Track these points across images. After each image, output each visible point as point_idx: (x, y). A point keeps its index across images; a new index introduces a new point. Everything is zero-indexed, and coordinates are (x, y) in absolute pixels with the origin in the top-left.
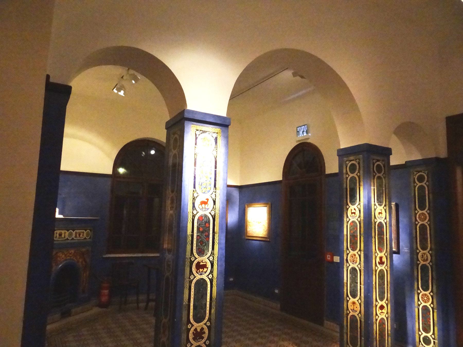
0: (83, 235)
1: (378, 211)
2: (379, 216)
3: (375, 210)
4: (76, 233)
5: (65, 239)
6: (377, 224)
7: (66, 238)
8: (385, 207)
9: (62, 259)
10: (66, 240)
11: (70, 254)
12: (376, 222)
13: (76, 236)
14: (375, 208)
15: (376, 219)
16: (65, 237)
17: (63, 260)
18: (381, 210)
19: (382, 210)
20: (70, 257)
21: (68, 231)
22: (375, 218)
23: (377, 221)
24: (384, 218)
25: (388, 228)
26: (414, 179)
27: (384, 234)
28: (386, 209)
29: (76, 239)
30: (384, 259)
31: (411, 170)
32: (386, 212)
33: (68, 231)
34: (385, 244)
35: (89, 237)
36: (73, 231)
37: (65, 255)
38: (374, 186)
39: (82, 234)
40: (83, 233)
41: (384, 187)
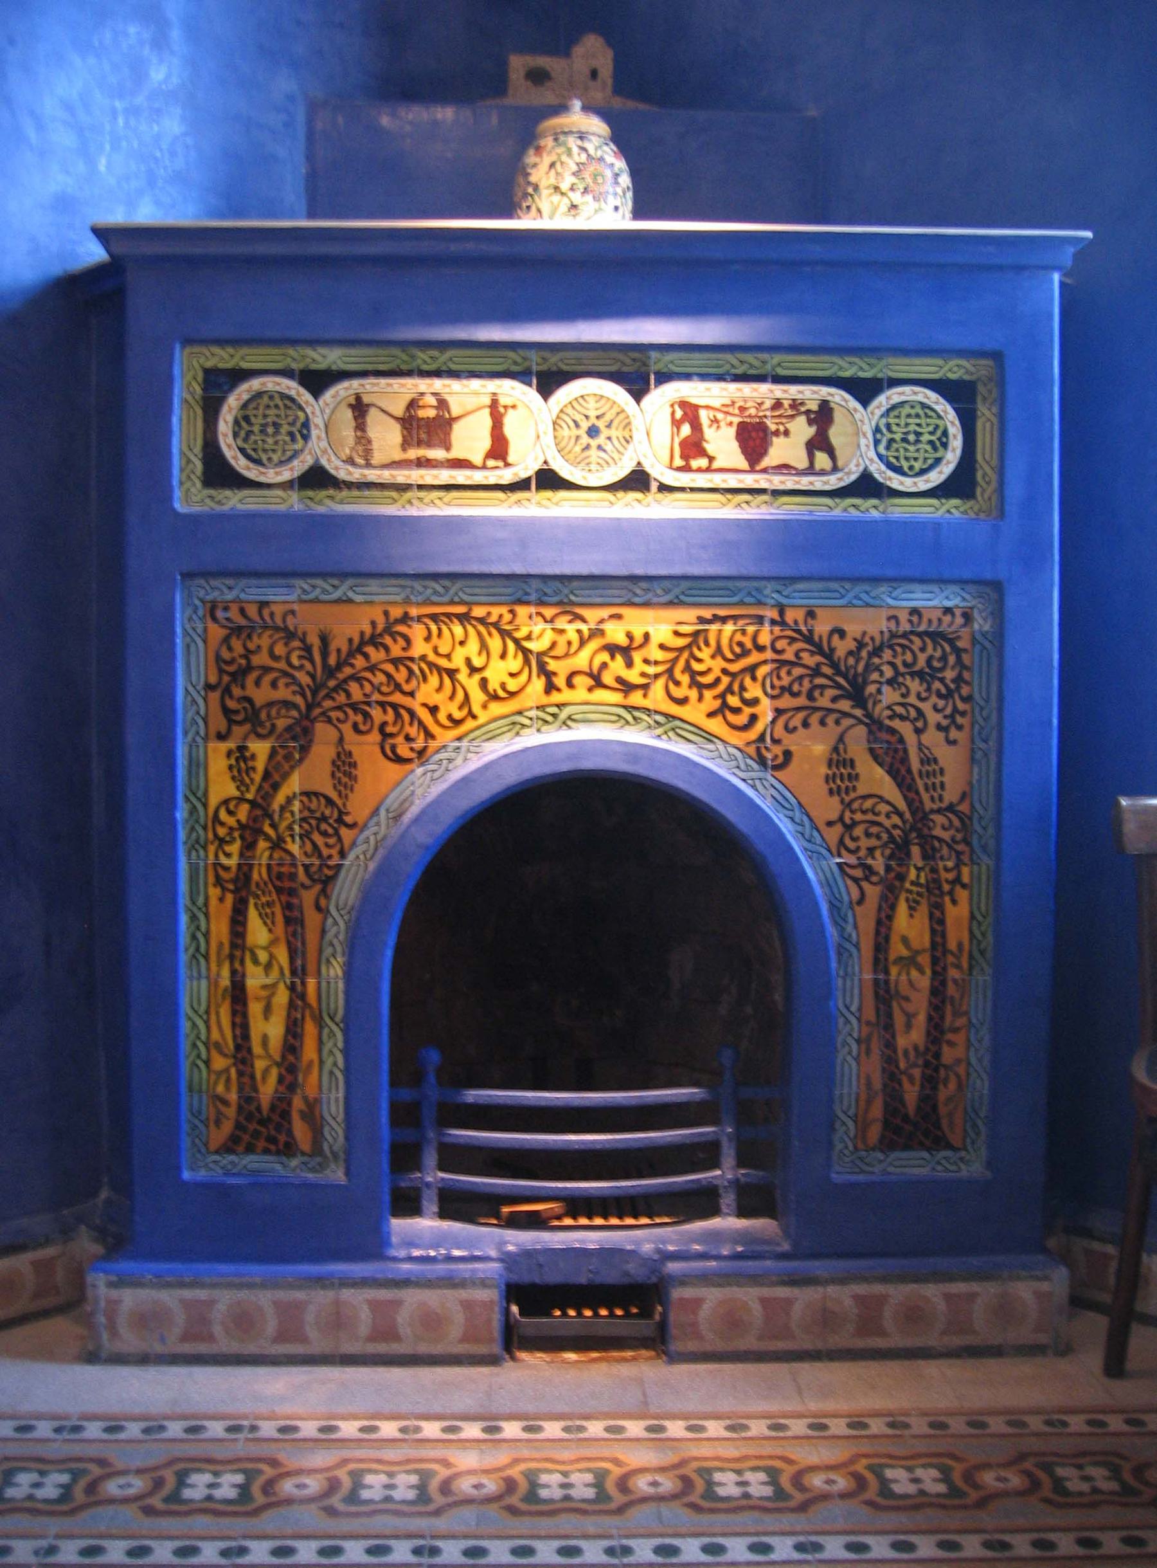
0: (820, 443)
4: (689, 412)
5: (506, 476)
7: (524, 463)
9: (495, 697)
10: (521, 485)
11: (625, 651)
13: (693, 448)
16: (499, 449)
17: (496, 709)
20: (626, 687)
21: (546, 391)
29: (664, 488)
33: (546, 391)
35: (935, 478)
36: (638, 395)
37: (540, 664)
39: (802, 430)
40: (823, 416)
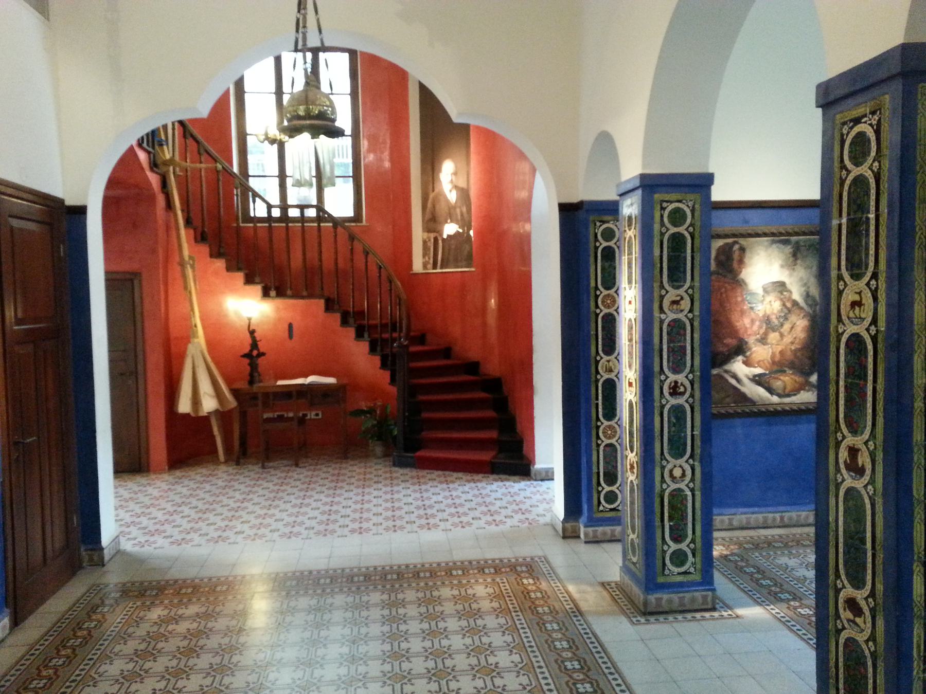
1: (849, 296)
2: (851, 315)
3: (840, 293)
6: (844, 339)
8: (873, 282)
12: (843, 333)
14: (841, 288)
15: (844, 324)
18: (860, 293)
19: (862, 294)
22: (840, 320)
23: (845, 331)
24: (870, 319)
25: (880, 356)
26: (596, 235)
27: (866, 375)
28: (877, 288)
30: (864, 459)
31: (591, 218)
32: (875, 299)
34: (870, 411)
38: (840, 215)
41: (873, 208)
